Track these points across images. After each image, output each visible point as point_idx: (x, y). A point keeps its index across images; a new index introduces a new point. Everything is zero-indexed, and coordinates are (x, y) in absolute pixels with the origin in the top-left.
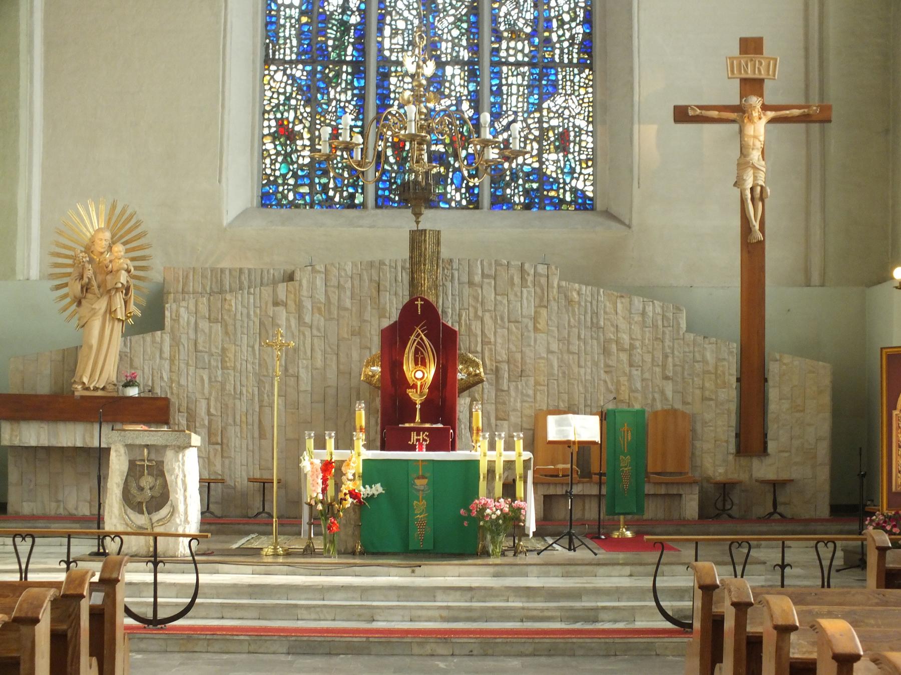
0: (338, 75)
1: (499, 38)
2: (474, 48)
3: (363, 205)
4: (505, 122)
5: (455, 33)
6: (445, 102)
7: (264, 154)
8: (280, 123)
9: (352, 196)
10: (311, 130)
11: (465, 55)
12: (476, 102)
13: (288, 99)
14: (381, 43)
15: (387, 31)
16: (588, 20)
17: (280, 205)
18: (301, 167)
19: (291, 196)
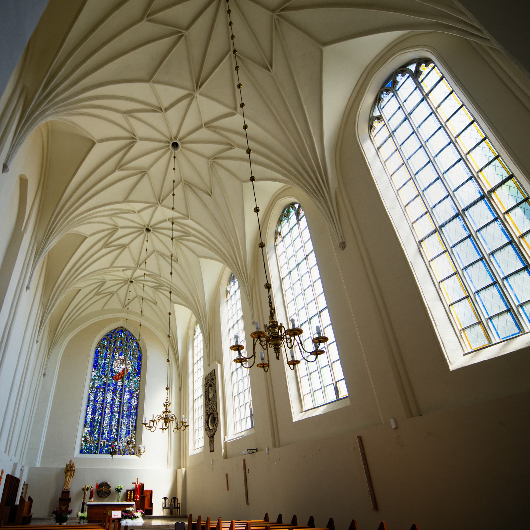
0: (96, 430)
1: (122, 425)
2: (118, 427)
3: (97, 454)
4: (121, 439)
5: (115, 424)
6: (112, 436)
7: (82, 444)
8: (85, 438)
9: (95, 452)
10: (90, 440)
11: (116, 427)
12: (117, 435)
13: (87, 434)
14: (103, 425)
15: (104, 423)
16: (136, 423)
17: (83, 453)
18: (88, 446)
19: (85, 452)
